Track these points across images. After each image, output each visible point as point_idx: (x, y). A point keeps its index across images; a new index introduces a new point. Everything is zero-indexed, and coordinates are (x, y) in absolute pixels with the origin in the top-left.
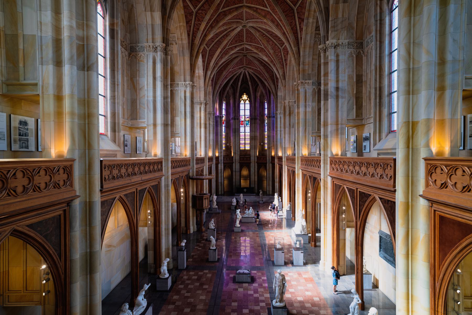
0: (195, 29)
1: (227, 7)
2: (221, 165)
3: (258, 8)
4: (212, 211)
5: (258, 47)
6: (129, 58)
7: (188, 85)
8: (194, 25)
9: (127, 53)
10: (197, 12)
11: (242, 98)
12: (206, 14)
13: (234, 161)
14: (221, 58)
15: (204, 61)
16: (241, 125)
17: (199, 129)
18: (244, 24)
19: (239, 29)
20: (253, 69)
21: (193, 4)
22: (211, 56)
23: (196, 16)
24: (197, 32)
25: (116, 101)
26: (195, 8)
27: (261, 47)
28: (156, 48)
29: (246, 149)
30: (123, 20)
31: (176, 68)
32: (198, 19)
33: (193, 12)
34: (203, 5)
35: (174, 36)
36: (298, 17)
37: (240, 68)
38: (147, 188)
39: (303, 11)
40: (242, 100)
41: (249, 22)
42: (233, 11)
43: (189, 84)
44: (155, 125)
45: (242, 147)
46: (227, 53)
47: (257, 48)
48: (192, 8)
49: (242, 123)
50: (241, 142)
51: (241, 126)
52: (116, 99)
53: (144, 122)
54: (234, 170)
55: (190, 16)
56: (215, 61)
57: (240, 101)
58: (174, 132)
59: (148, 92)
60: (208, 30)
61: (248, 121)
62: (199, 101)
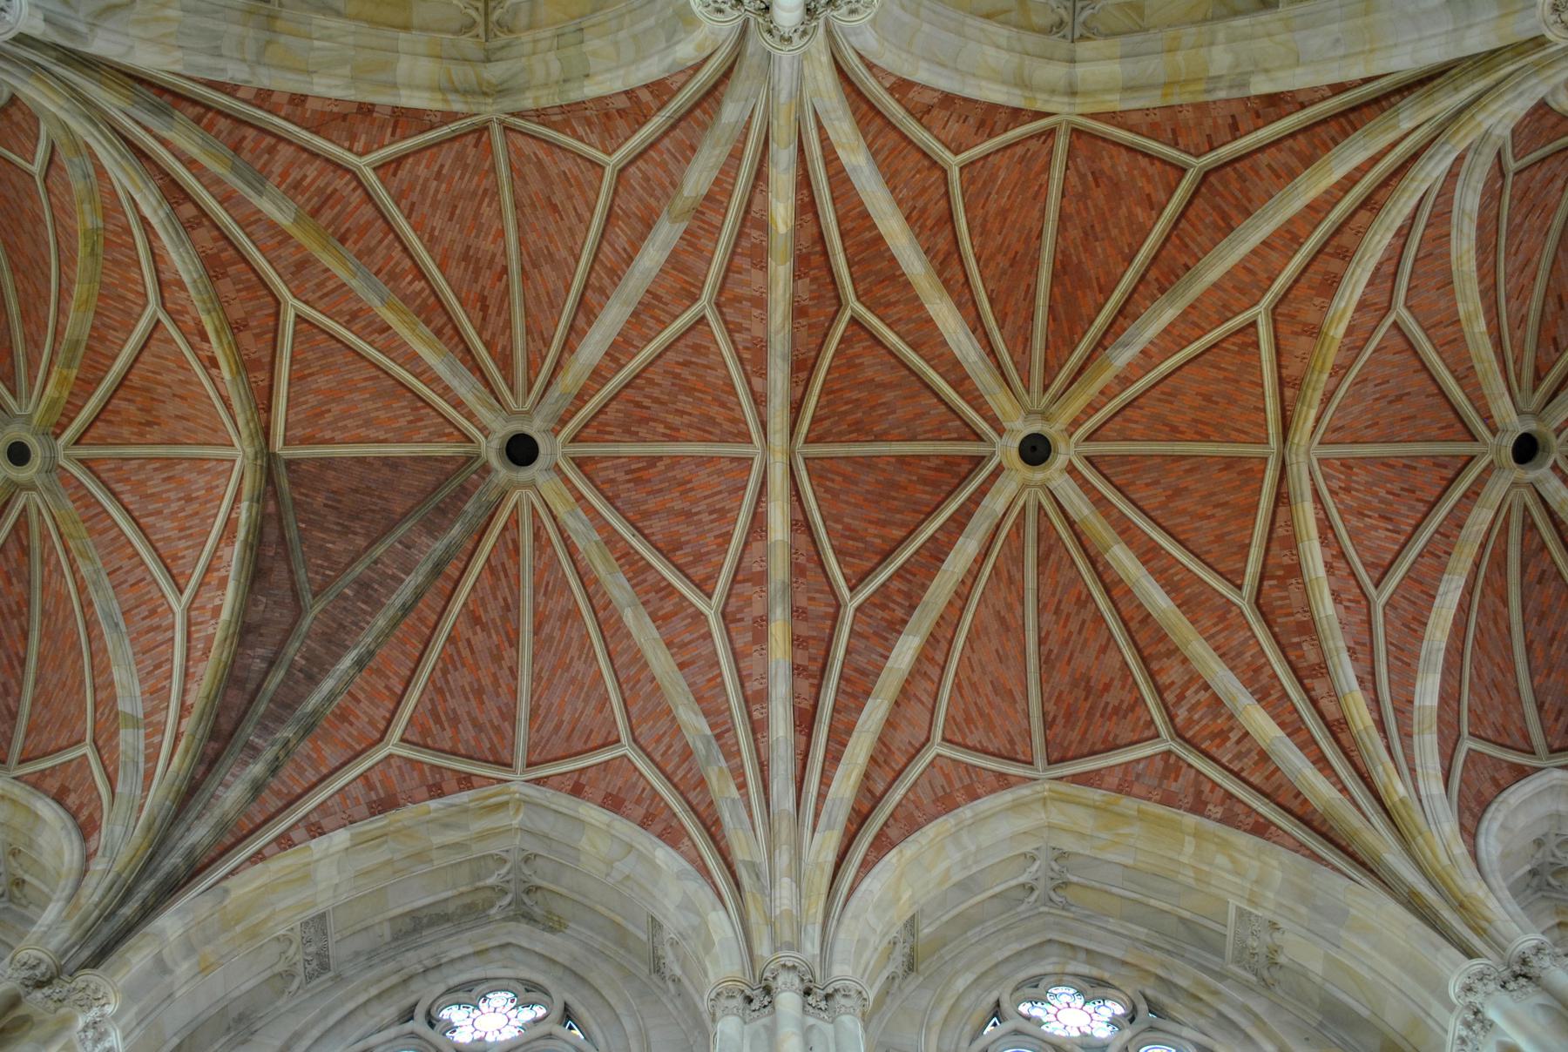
0: (1256, 779)
1: (1247, 556)
3: (1280, 378)
8: (1231, 771)
10: (1179, 735)
12: (1206, 687)
21: (1135, 738)
23: (1190, 743)
24: (1278, 769)
26: (1157, 735)
32: (1213, 736)
33: (1169, 753)
34: (1159, 691)
36: (1235, 139)
39: (1188, 115)
41: (1487, 419)
42: (1291, 523)
55: (1176, 780)
60: (1314, 702)
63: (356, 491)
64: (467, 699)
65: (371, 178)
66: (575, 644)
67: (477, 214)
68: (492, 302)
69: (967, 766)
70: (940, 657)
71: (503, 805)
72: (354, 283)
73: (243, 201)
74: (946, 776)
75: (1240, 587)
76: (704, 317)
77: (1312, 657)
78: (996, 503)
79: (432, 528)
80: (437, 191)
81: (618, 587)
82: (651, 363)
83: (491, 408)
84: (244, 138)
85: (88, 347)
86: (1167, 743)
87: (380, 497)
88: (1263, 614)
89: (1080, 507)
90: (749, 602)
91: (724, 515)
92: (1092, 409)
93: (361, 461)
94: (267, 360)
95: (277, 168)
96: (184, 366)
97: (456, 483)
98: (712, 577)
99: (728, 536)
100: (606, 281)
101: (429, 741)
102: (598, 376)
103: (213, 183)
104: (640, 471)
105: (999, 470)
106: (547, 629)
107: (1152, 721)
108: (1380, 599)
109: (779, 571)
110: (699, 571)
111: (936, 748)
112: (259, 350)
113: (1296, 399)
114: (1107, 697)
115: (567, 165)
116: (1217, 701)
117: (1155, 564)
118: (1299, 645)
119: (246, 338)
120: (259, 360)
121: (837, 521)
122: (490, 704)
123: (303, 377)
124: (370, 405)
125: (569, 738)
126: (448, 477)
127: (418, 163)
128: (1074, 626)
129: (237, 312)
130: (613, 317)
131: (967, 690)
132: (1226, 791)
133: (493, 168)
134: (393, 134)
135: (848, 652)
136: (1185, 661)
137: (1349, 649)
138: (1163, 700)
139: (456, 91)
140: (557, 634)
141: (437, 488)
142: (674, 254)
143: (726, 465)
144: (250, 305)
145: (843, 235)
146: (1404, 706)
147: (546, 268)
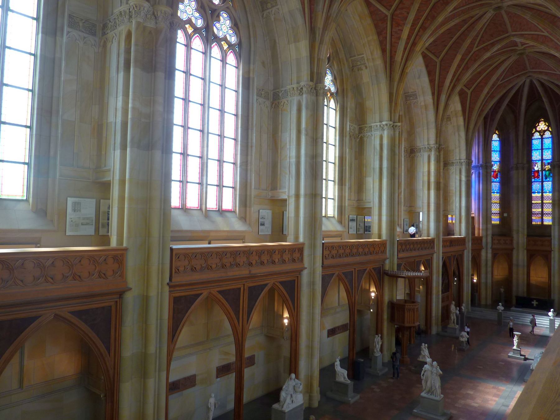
2: (487, 253)
4: (446, 332)
5: (538, 35)
6: (271, 109)
7: (385, 127)
9: (268, 103)
10: (393, 15)
11: (536, 128)
12: (408, 13)
13: (515, 245)
14: (467, 68)
15: (432, 81)
16: (534, 178)
17: (426, 192)
18: (496, 6)
19: (489, 15)
20: (547, 74)
22: (445, 69)
23: (392, 19)
24: (398, 43)
25: (249, 168)
26: (389, 10)
27: (543, 36)
28: (301, 90)
29: (546, 223)
30: (263, 63)
31: (369, 104)
33: (387, 16)
35: (362, 57)
37: (518, 76)
38: (266, 285)
40: (536, 131)
43: (387, 125)
44: (297, 196)
45: (536, 220)
47: (536, 38)
49: (536, 174)
50: (533, 210)
51: (533, 180)
52: (249, 165)
53: (285, 193)
54: (514, 262)
56: (454, 76)
57: (533, 135)
58: (363, 200)
59: (290, 151)
60: (417, 35)
61: (548, 170)
62: (426, 146)
86: (388, 14)
116: (406, 18)
138: (399, 4)
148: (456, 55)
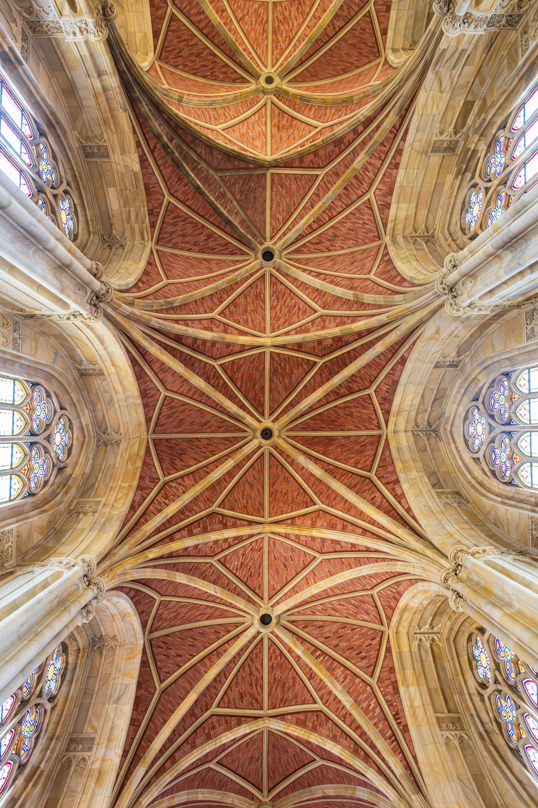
10: (166, 483)
26: (165, 476)
32: (166, 494)
33: (159, 480)
34: (182, 477)
42: (242, 526)
46: (212, 732)
48: (160, 472)
60: (179, 530)
63: (255, 198)
64: (181, 231)
65: (365, 198)
66: (200, 271)
67: (350, 239)
68: (318, 246)
69: (156, 405)
70: (196, 397)
71: (143, 238)
72: (330, 193)
73: (362, 149)
74: (152, 396)
75: (219, 507)
76: (316, 312)
77: (195, 531)
78: (249, 419)
79: (242, 222)
80: (359, 223)
81: (221, 283)
82: (299, 298)
83: (283, 245)
84: (385, 146)
85: (307, 105)
86: (162, 480)
87: (252, 207)
88: (210, 514)
89: (247, 450)
90: (218, 327)
91: (246, 322)
92: (281, 453)
93: (265, 201)
94: (303, 165)
95: (373, 161)
96: (301, 137)
97: (257, 233)
98: (225, 317)
99: (239, 323)
100: (328, 280)
101: (168, 213)
102: (294, 280)
103: (370, 137)
104: (260, 297)
105: (260, 422)
106: (205, 263)
107: (170, 474)
108: (213, 561)
109: (230, 338)
110: (227, 312)
111: (164, 393)
112: (307, 161)
113: (287, 524)
114: (178, 460)
115: (368, 265)
117: (227, 477)
118: (200, 527)
119: (312, 157)
120: (303, 162)
121: (243, 362)
122: (179, 239)
123: (296, 179)
124: (284, 204)
125: (167, 264)
126: (259, 231)
127: (369, 215)
128: (203, 450)
129: (321, 153)
130: (316, 283)
131: (183, 408)
132: (146, 498)
133: (366, 243)
134: (381, 205)
135: (200, 360)
136: (193, 485)
137: (198, 545)
139: (394, 226)
140: (203, 265)
141: (255, 226)
142: (341, 298)
143: (263, 325)
144: (323, 157)
145: (348, 352)
146: (175, 567)
147: (331, 263)
148: (188, 692)
